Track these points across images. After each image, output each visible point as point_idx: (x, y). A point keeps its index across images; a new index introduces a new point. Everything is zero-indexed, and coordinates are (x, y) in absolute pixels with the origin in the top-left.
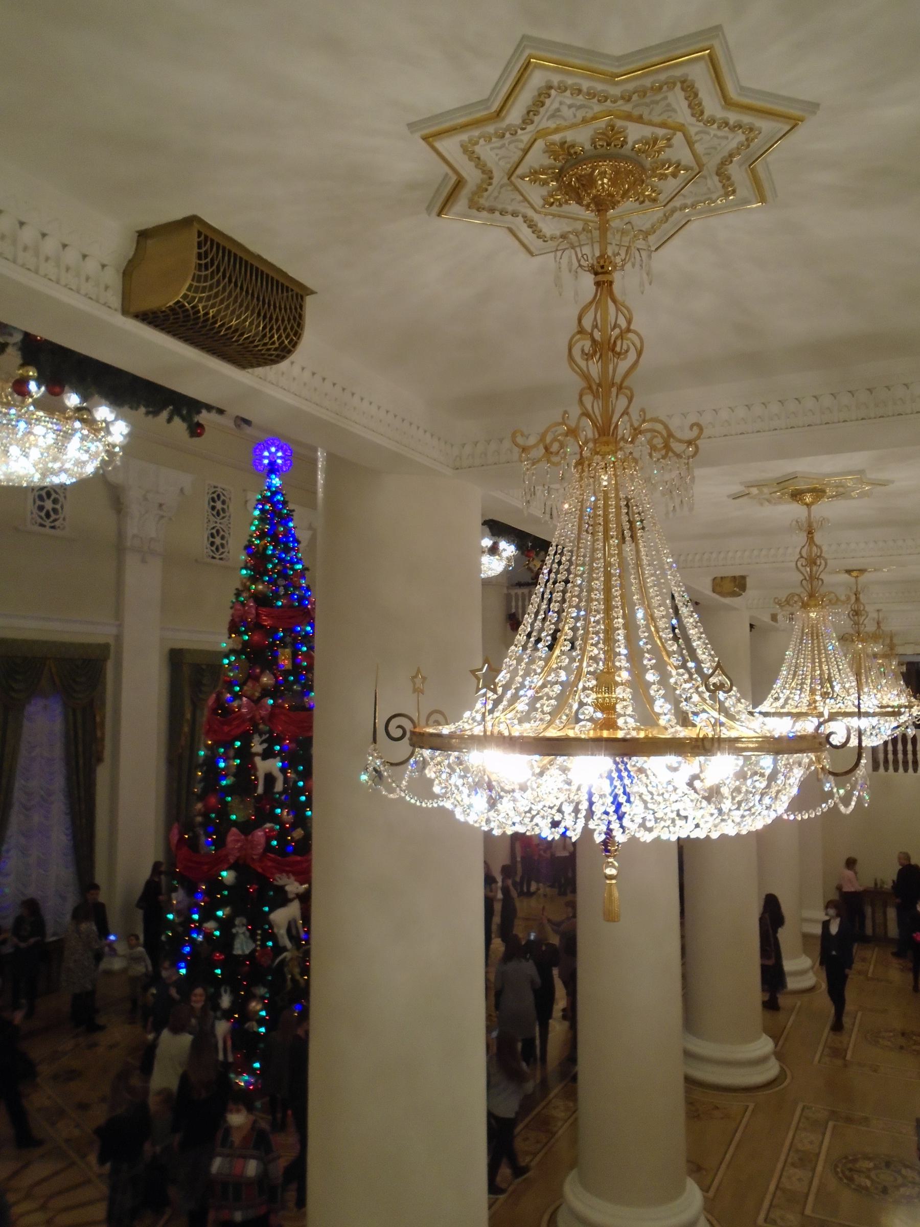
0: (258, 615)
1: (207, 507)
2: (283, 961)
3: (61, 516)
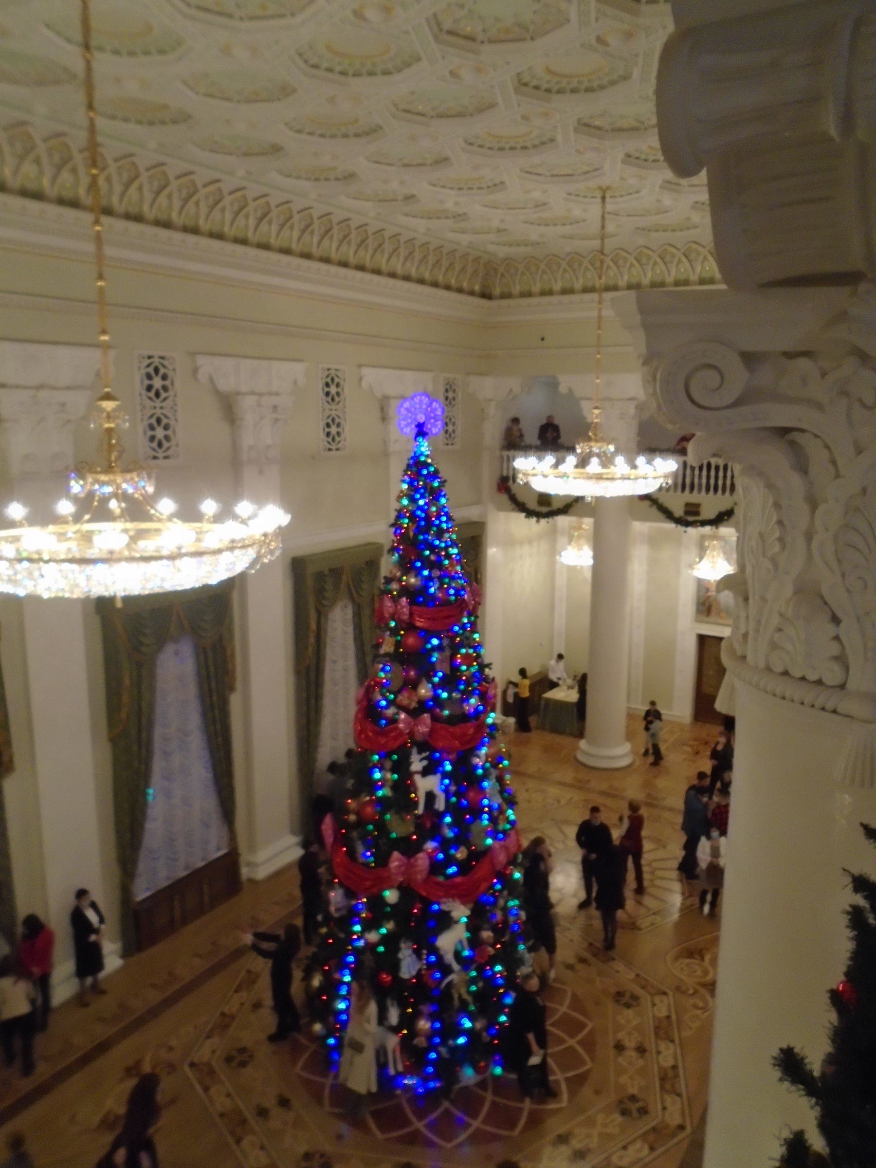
0: (411, 614)
1: (321, 395)
2: (450, 984)
3: (173, 442)
